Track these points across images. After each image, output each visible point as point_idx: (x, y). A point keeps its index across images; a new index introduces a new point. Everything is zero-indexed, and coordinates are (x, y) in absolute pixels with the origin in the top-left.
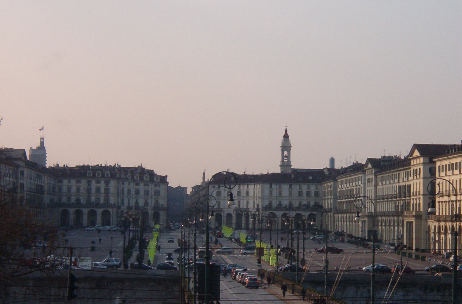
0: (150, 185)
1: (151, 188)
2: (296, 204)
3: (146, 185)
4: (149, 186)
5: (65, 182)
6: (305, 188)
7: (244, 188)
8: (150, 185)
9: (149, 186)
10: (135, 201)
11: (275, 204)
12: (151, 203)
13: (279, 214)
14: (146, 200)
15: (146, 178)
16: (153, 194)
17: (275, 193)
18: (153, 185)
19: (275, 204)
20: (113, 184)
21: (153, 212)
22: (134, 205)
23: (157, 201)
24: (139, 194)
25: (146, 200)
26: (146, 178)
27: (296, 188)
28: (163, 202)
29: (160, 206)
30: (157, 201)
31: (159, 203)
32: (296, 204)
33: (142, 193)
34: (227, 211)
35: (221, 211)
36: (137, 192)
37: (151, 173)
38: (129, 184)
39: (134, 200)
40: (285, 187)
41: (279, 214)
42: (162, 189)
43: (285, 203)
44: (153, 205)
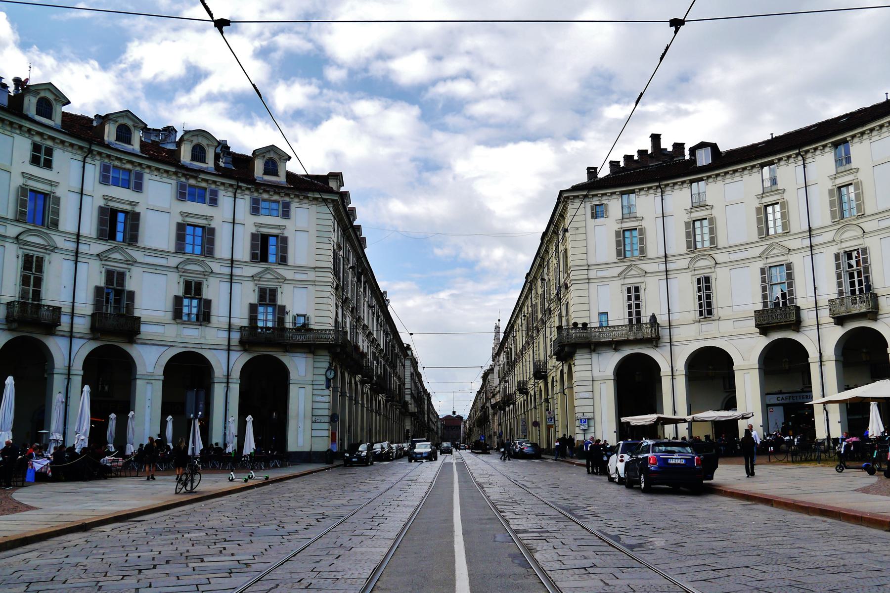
0: (225, 199)
3: (197, 195)
4: (214, 202)
8: (225, 199)
9: (214, 202)
10: (101, 281)
12: (232, 302)
14: (193, 289)
16: (243, 251)
18: (244, 203)
21: (239, 360)
22: (85, 305)
23: (267, 297)
24: (132, 238)
25: (193, 289)
29: (289, 324)
30: (267, 297)
31: (282, 310)
33: (157, 232)
34: (689, 338)
35: (654, 341)
36: (119, 225)
38: (41, 157)
39: (92, 276)
42: (307, 231)
44: (241, 318)
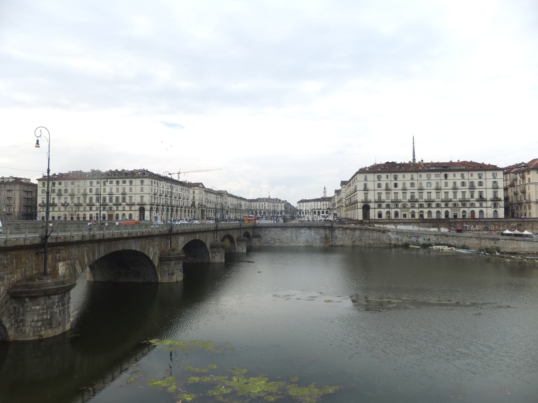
1: (280, 205)
2: (322, 208)
5: (252, 203)
6: (325, 203)
7: (307, 203)
11: (316, 208)
13: (317, 211)
15: (278, 201)
17: (316, 204)
19: (316, 208)
20: (266, 203)
26: (278, 201)
27: (322, 203)
28: (283, 209)
32: (322, 208)
37: (280, 200)
40: (319, 203)
41: (317, 211)
43: (319, 208)
